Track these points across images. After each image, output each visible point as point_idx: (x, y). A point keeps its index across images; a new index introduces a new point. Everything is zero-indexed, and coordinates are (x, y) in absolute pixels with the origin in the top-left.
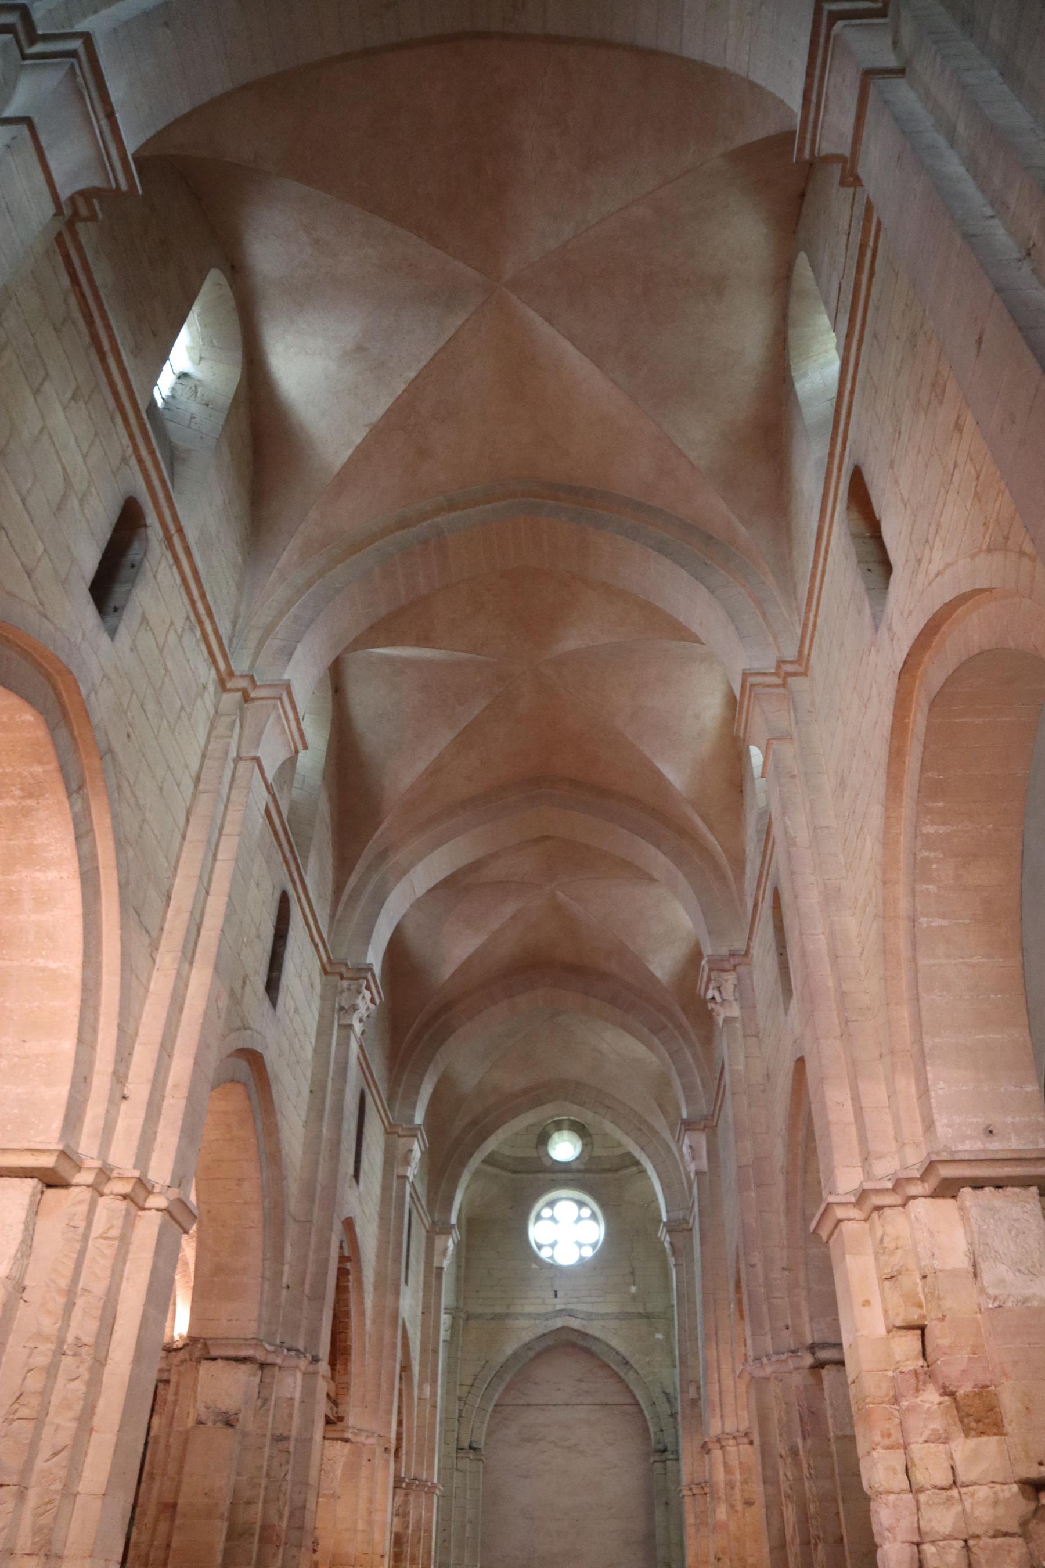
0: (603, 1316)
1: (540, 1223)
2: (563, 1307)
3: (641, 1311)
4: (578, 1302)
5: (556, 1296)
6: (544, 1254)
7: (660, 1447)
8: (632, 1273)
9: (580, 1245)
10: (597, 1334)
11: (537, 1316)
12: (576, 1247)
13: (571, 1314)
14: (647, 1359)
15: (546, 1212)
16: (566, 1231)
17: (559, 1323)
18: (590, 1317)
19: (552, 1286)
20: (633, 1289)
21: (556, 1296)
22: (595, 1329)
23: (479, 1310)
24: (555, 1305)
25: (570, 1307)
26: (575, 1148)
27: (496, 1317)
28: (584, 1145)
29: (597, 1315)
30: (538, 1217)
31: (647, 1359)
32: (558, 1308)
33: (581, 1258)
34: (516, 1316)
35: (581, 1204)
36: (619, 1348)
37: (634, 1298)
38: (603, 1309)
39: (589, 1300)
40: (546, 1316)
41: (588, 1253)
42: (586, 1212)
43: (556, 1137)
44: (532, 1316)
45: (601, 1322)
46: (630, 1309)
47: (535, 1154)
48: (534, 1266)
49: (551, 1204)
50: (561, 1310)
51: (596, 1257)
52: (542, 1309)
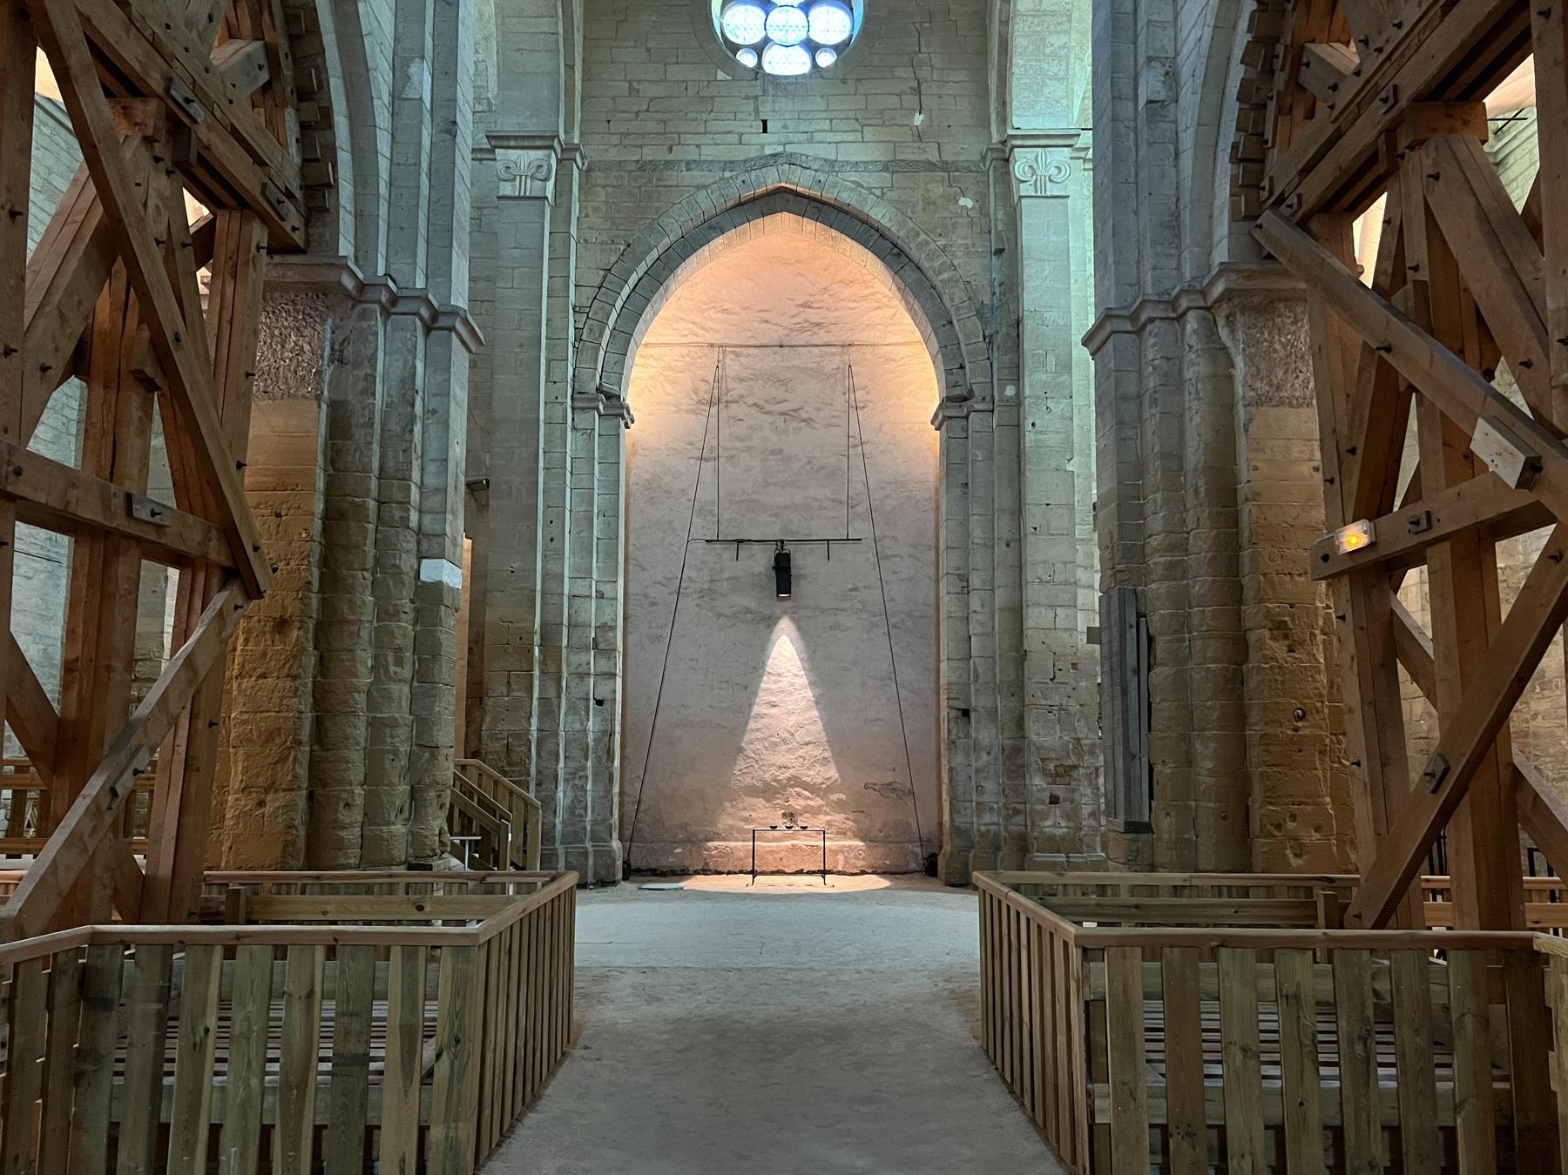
2: (780, 149)
3: (933, 156)
4: (810, 141)
5: (765, 131)
7: (958, 391)
10: (845, 198)
11: (728, 165)
14: (942, 242)
18: (832, 165)
19: (757, 112)
20: (918, 119)
21: (765, 131)
23: (613, 155)
24: (763, 146)
25: (790, 149)
27: (642, 167)
31: (942, 242)
32: (769, 151)
36: (886, 222)
37: (919, 137)
39: (830, 137)
45: (853, 177)
46: (911, 154)
48: (721, 75)
50: (775, 155)
52: (739, 154)
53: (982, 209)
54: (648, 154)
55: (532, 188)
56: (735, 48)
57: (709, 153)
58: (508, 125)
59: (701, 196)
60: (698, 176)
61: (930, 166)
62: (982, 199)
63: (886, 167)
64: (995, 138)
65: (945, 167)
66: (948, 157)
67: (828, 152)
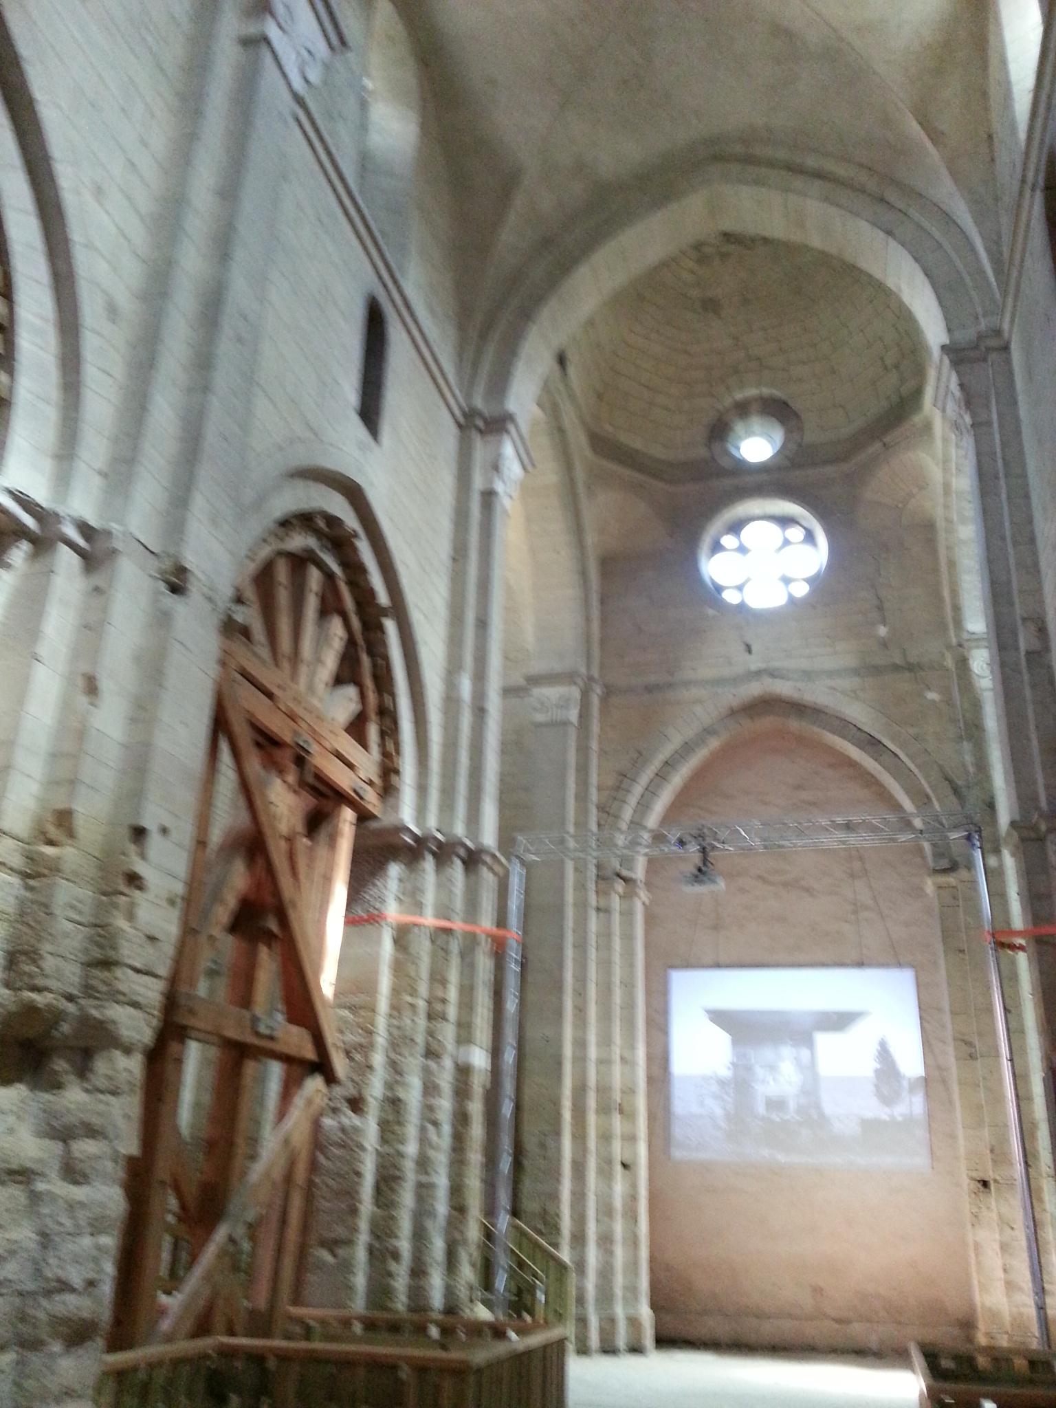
0: (831, 674)
1: (719, 556)
3: (898, 660)
6: (731, 597)
8: (880, 608)
9: (787, 581)
11: (719, 682)
12: (782, 585)
13: (773, 674)
14: (912, 731)
15: (728, 541)
16: (765, 562)
17: (755, 689)
18: (808, 675)
20: (882, 631)
21: (750, 651)
22: (817, 694)
26: (770, 438)
27: (649, 689)
28: (788, 433)
29: (825, 676)
30: (717, 547)
31: (912, 731)
33: (792, 599)
34: (687, 684)
35: (785, 521)
37: (884, 644)
38: (829, 663)
40: (736, 680)
41: (801, 590)
42: (796, 533)
43: (739, 427)
44: (713, 680)
47: (702, 452)
48: (711, 612)
49: (735, 528)
51: (813, 592)
52: (726, 672)
53: (949, 702)
54: (653, 679)
55: (559, 715)
56: (719, 589)
57: (705, 672)
58: (538, 666)
59: (698, 709)
60: (695, 692)
61: (896, 668)
62: (946, 691)
63: (856, 672)
64: (954, 641)
65: (910, 668)
66: (913, 659)
67: (804, 664)
